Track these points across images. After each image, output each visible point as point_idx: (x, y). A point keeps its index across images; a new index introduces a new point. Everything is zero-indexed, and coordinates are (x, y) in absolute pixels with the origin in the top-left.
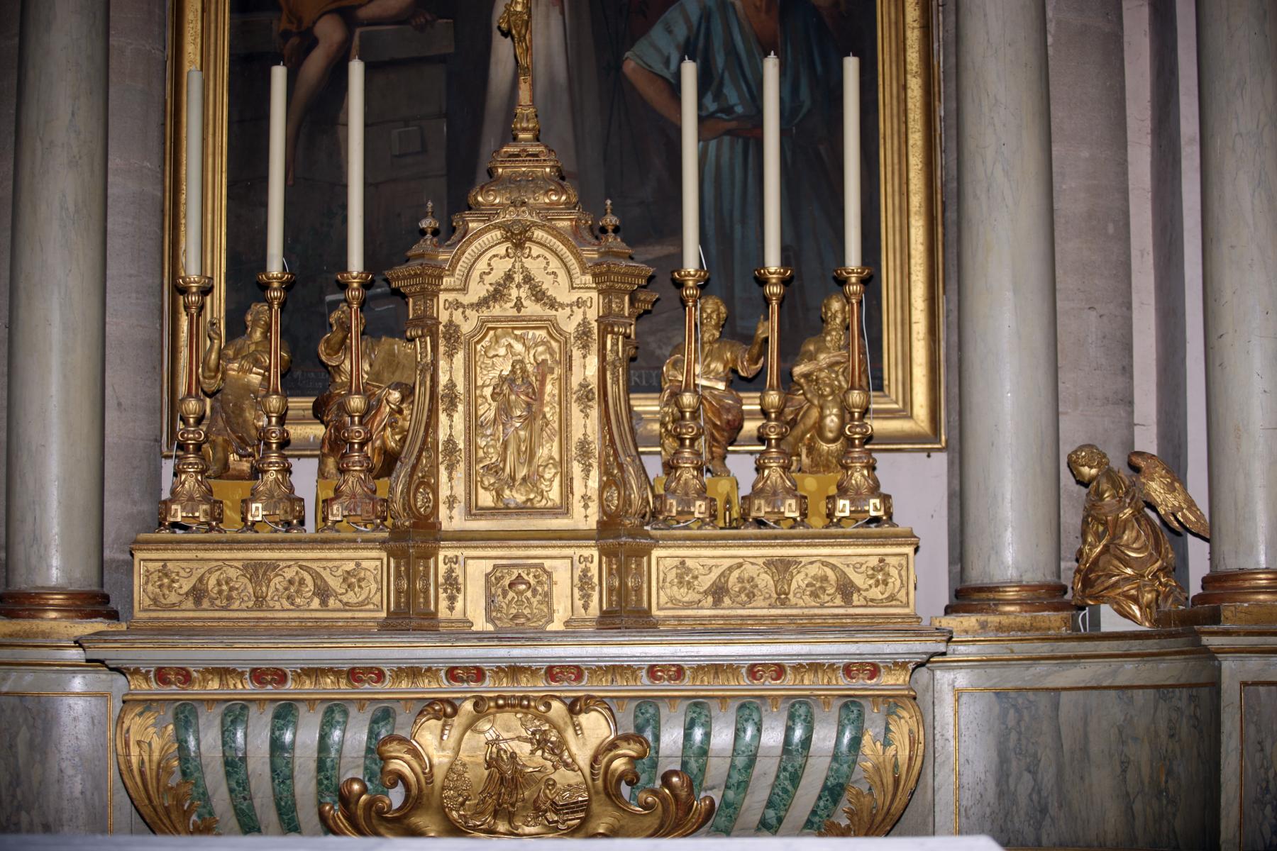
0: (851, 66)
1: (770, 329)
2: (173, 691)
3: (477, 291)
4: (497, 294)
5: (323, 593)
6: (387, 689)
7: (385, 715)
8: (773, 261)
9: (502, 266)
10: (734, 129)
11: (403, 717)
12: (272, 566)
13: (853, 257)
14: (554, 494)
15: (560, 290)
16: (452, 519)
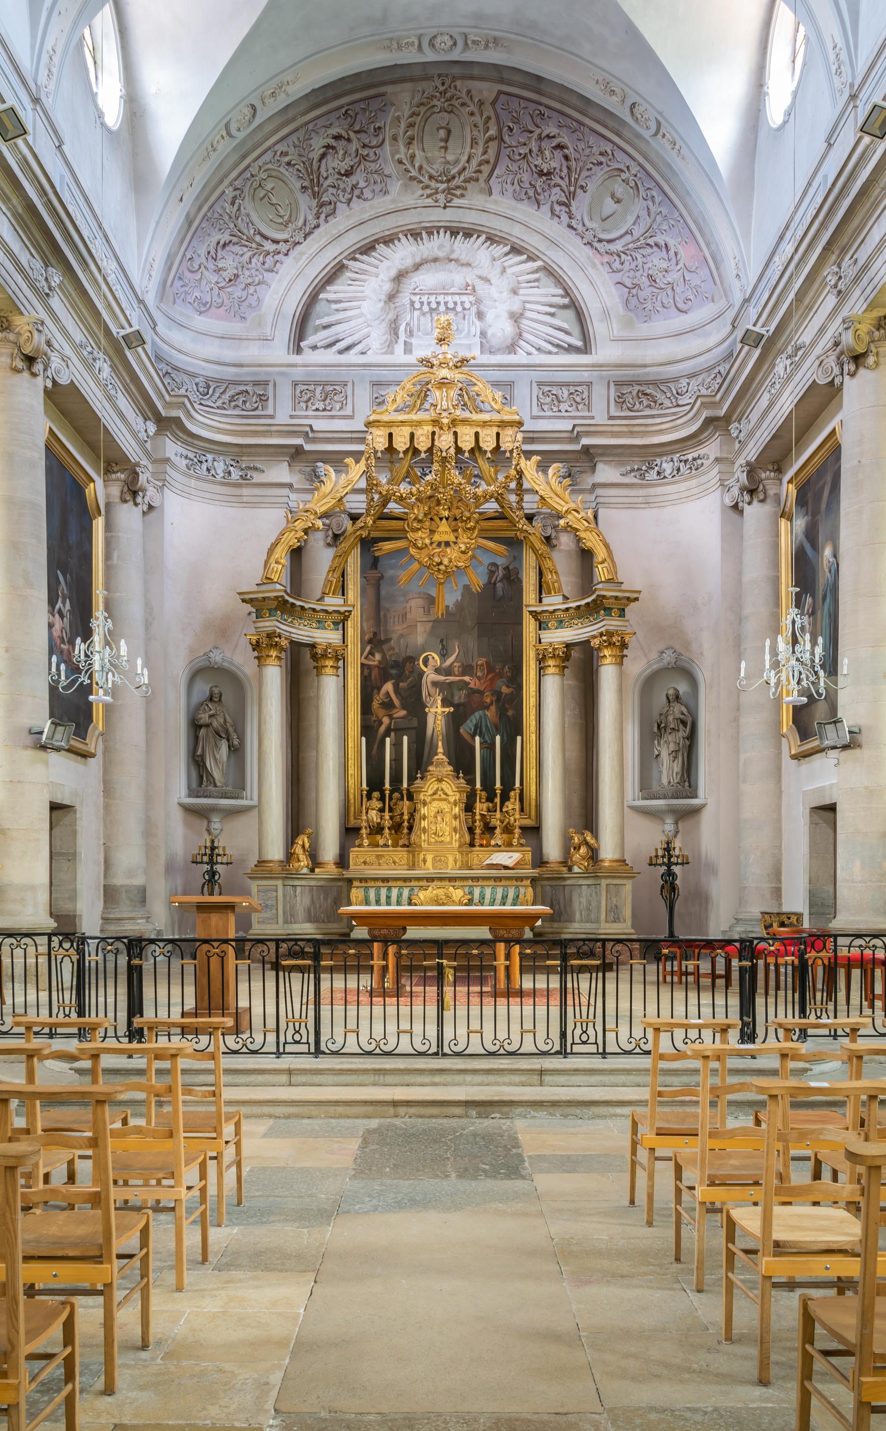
0: (519, 738)
1: (498, 800)
2: (363, 884)
3: (430, 792)
4: (434, 794)
5: (394, 862)
6: (413, 883)
7: (412, 890)
8: (498, 785)
9: (436, 787)
10: (489, 747)
11: (416, 890)
12: (382, 856)
13: (517, 784)
14: (448, 839)
15: (449, 792)
16: (424, 845)
